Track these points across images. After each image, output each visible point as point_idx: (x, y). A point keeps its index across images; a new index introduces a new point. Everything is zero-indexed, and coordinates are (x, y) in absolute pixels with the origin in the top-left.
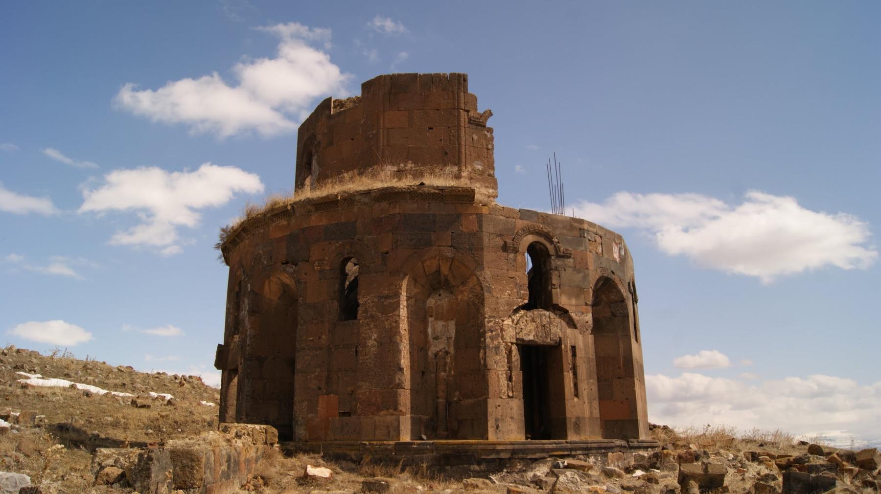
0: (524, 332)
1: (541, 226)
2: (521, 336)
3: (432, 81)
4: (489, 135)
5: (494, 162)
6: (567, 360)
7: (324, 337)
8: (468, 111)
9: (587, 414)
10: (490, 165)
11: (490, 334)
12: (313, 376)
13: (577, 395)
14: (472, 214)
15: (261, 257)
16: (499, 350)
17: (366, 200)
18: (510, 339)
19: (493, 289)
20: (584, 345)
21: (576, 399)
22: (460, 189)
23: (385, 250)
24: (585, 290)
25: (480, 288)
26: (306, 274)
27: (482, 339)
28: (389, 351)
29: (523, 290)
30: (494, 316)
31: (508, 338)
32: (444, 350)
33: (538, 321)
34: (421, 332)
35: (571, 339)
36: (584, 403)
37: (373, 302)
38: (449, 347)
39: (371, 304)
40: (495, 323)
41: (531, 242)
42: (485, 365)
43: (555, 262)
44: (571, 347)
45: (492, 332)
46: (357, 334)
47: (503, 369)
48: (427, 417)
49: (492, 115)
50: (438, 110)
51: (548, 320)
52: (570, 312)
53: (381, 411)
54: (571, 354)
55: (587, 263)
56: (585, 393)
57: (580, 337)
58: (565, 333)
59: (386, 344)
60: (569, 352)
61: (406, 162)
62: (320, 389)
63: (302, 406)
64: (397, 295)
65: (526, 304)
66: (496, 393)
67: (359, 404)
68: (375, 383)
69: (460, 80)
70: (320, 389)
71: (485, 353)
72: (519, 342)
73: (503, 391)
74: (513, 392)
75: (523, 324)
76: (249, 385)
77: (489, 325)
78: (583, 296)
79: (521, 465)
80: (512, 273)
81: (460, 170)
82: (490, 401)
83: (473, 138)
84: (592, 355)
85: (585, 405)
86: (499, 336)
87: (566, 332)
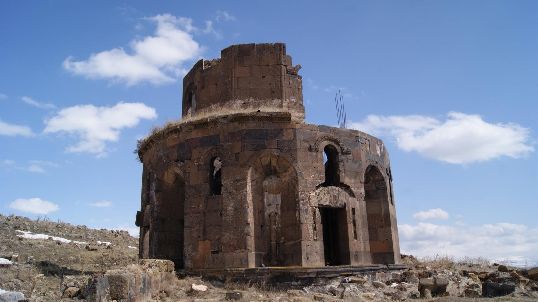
0: (323, 200)
1: (332, 135)
2: (321, 202)
3: (264, 48)
4: (299, 80)
5: (302, 97)
6: (350, 217)
7: (201, 205)
8: (286, 66)
9: (362, 249)
10: (301, 99)
11: (302, 201)
12: (195, 229)
13: (356, 238)
14: (289, 129)
15: (162, 158)
16: (308, 211)
17: (225, 122)
18: (315, 204)
19: (303, 174)
20: (360, 207)
21: (355, 240)
22: (282, 114)
23: (237, 152)
24: (360, 173)
25: (295, 174)
26: (189, 167)
27: (298, 205)
28: (241, 213)
29: (322, 175)
30: (305, 191)
31: (313, 204)
32: (274, 212)
33: (332, 193)
34: (260, 201)
35: (351, 204)
36: (361, 242)
37: (231, 184)
38: (277, 210)
39: (229, 185)
40: (305, 195)
41: (326, 145)
42: (300, 221)
43: (341, 157)
44: (352, 209)
45: (303, 200)
46: (221, 203)
47: (310, 223)
48: (264, 253)
49: (301, 68)
50: (268, 66)
51: (338, 192)
52: (351, 187)
53: (236, 250)
54: (352, 213)
55: (360, 157)
56: (361, 237)
57: (357, 202)
58: (348, 200)
59: (239, 209)
60: (351, 212)
61: (249, 98)
62: (199, 237)
63: (189, 248)
64: (245, 179)
65: (324, 183)
66: (306, 237)
67: (223, 246)
68: (233, 233)
69: (281, 47)
70: (199, 237)
71: (299, 213)
72: (320, 206)
73: (311, 236)
74: (317, 237)
75: (322, 195)
76: (157, 236)
77: (302, 196)
78: (358, 178)
79: (322, 281)
80: (315, 164)
81: (282, 102)
82: (303, 243)
83: (289, 82)
84: (365, 213)
85: (361, 244)
86: (308, 203)
87: (349, 199)
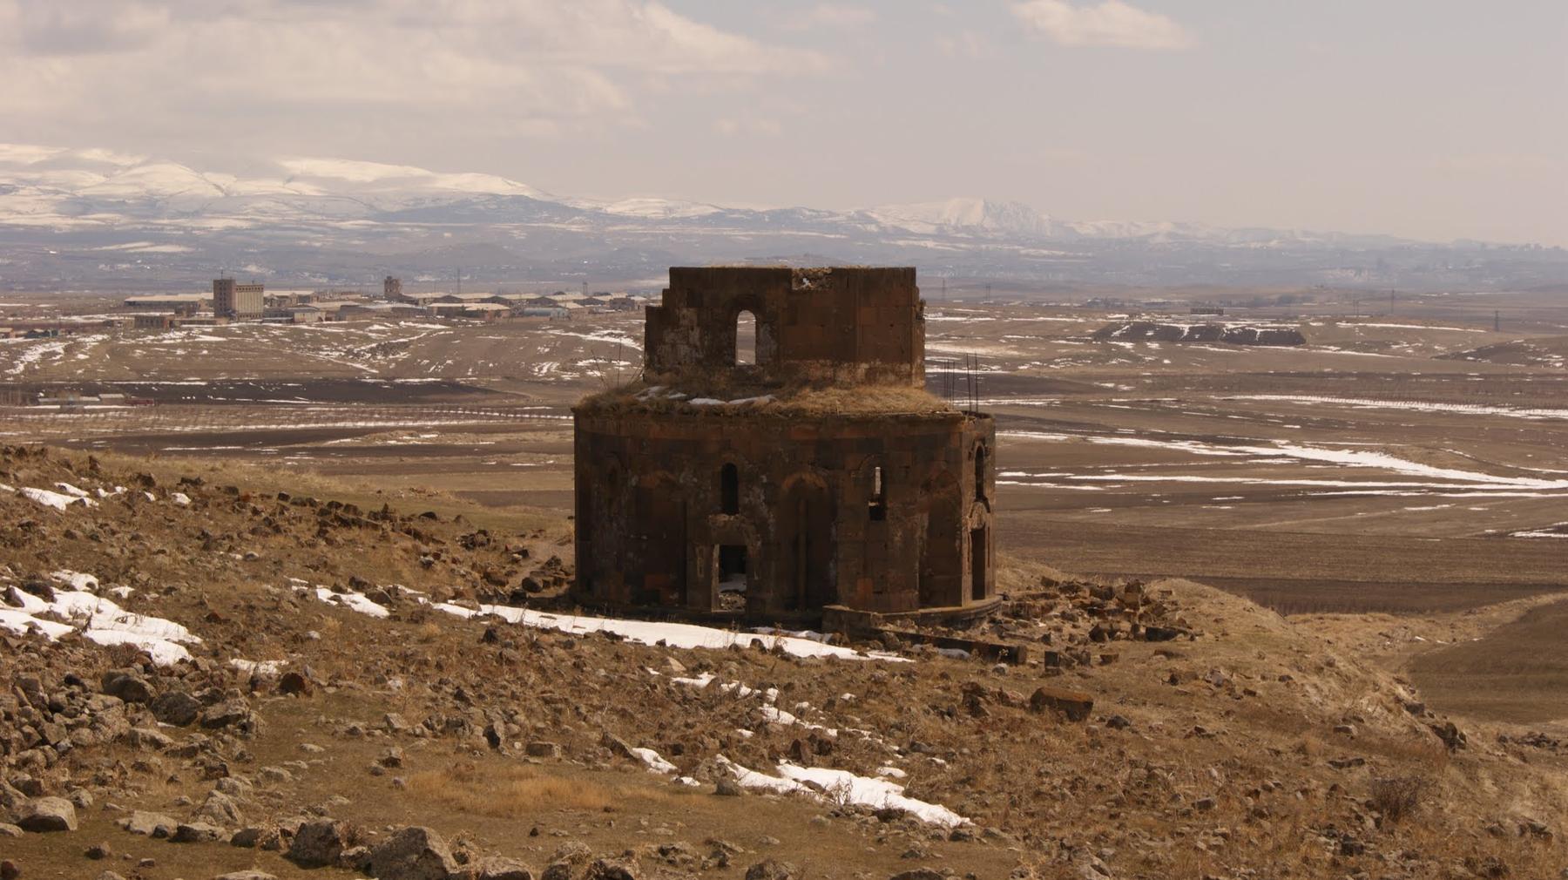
81: (911, 368)
